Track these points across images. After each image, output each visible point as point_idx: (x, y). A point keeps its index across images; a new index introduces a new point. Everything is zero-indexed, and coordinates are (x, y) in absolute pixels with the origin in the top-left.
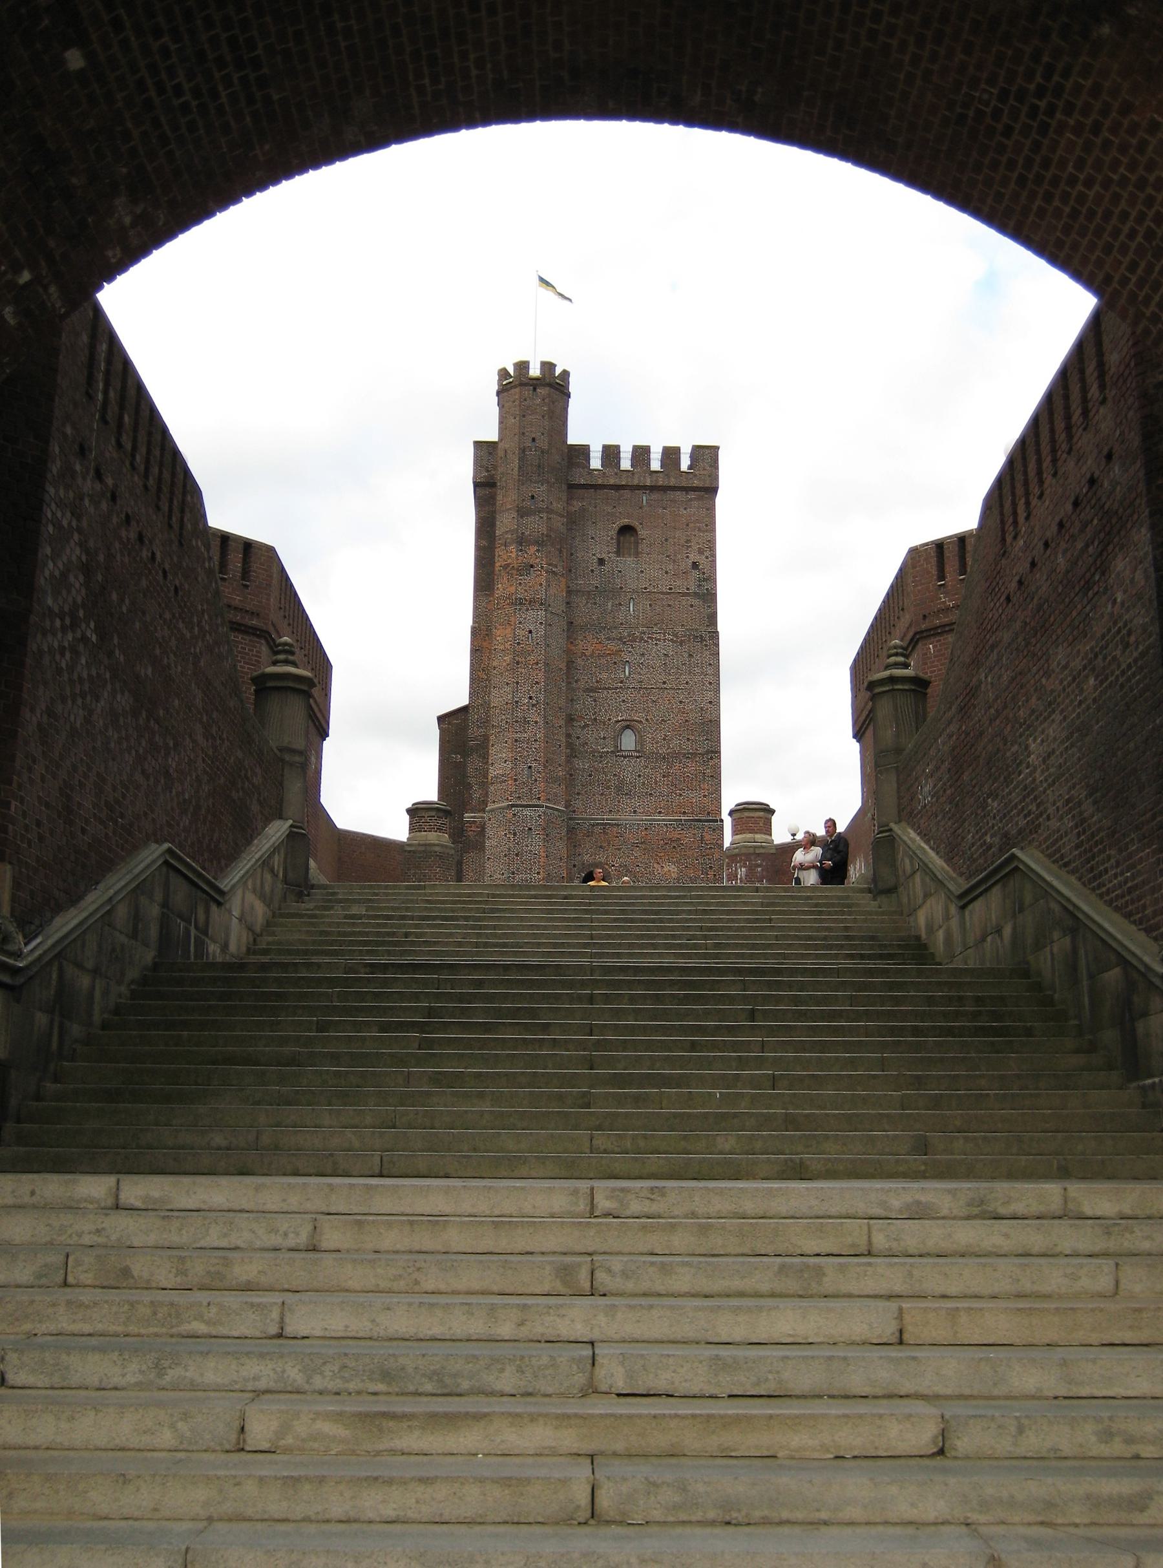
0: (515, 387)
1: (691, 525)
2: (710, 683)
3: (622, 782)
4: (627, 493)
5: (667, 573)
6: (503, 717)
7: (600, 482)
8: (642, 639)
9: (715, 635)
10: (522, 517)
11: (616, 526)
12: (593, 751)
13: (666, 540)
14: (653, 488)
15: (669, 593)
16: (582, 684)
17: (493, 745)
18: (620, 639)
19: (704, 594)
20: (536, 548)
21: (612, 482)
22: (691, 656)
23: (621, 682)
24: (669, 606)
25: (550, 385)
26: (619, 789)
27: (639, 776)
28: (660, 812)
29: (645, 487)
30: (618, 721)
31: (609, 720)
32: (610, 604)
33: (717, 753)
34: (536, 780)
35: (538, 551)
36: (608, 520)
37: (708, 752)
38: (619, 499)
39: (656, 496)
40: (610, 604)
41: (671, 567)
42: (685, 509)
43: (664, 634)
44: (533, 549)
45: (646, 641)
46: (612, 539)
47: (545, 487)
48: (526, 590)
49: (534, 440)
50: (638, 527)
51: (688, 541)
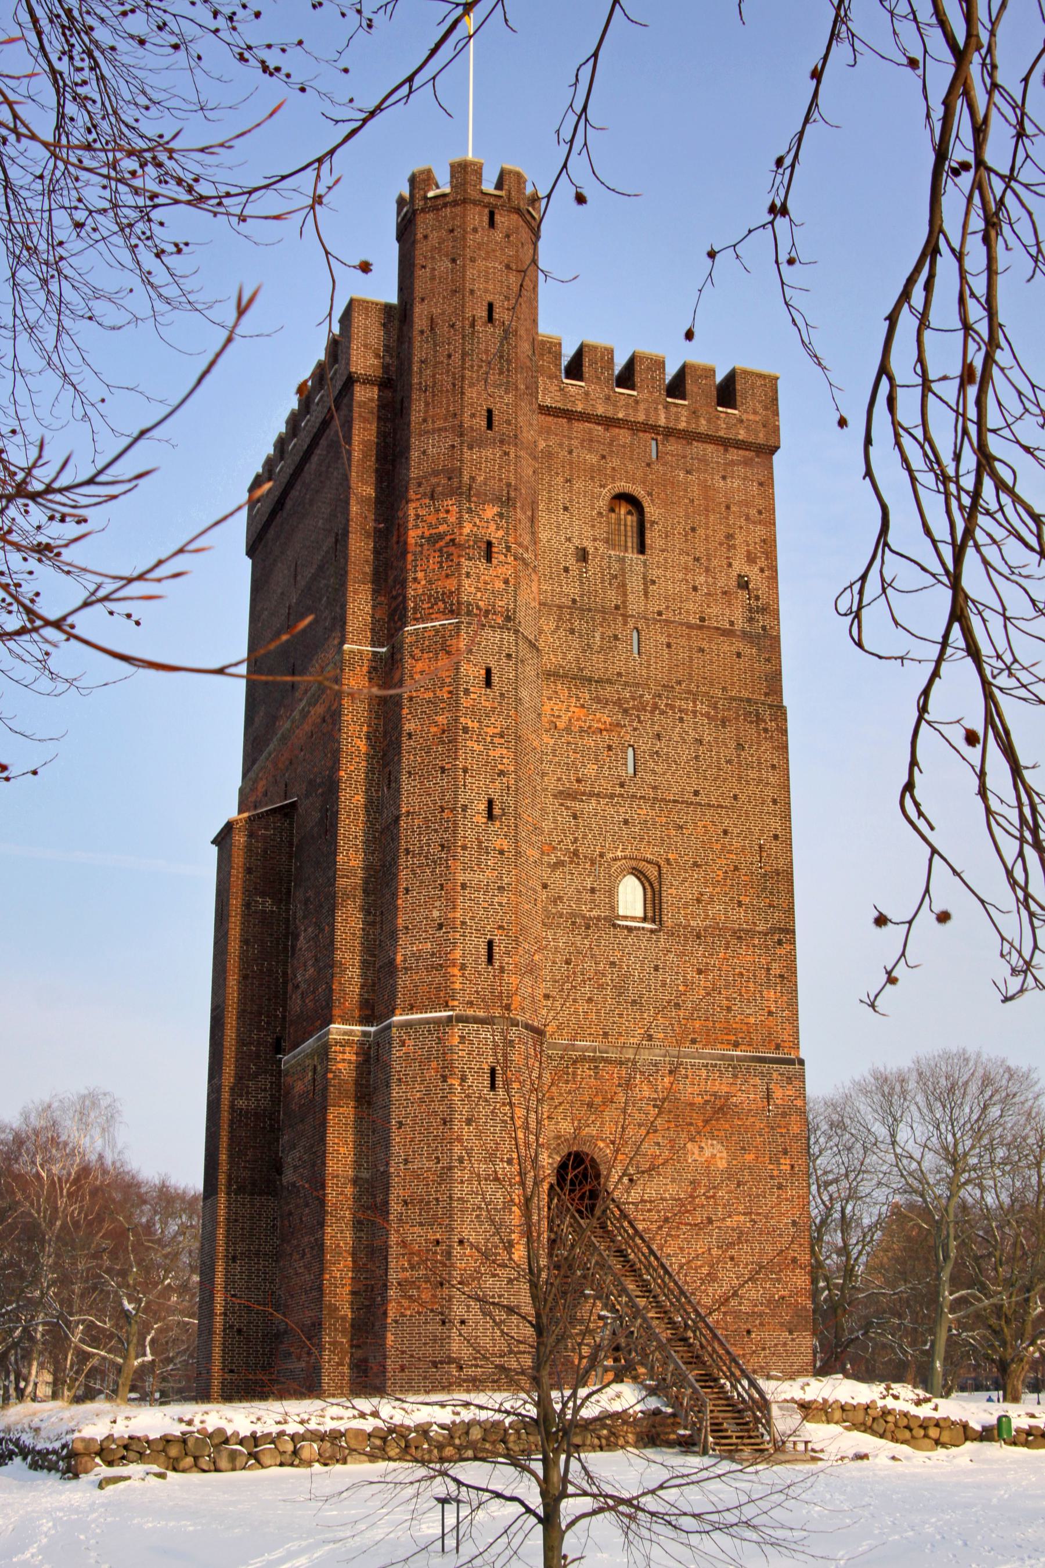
0: (455, 203)
1: (734, 508)
2: (775, 802)
3: (625, 977)
4: (624, 436)
5: (695, 589)
6: (434, 836)
7: (579, 408)
8: (655, 707)
9: (779, 713)
10: (471, 448)
11: (607, 493)
12: (573, 915)
13: (693, 529)
14: (670, 433)
15: (701, 628)
16: (551, 783)
17: (407, 890)
18: (618, 703)
20: (496, 510)
21: (600, 411)
22: (740, 747)
23: (622, 785)
24: (701, 650)
25: (518, 211)
26: (620, 990)
27: (656, 969)
28: (694, 1041)
29: (654, 429)
30: (615, 859)
31: (602, 855)
32: (597, 635)
33: (786, 933)
34: (502, 969)
35: (500, 515)
36: (592, 478)
37: (773, 931)
38: (611, 444)
39: (673, 446)
40: (597, 635)
41: (702, 579)
42: (724, 478)
43: (694, 702)
45: (662, 713)
46: (600, 514)
47: (509, 398)
48: (478, 589)
49: (490, 306)
50: (646, 502)
51: (730, 536)
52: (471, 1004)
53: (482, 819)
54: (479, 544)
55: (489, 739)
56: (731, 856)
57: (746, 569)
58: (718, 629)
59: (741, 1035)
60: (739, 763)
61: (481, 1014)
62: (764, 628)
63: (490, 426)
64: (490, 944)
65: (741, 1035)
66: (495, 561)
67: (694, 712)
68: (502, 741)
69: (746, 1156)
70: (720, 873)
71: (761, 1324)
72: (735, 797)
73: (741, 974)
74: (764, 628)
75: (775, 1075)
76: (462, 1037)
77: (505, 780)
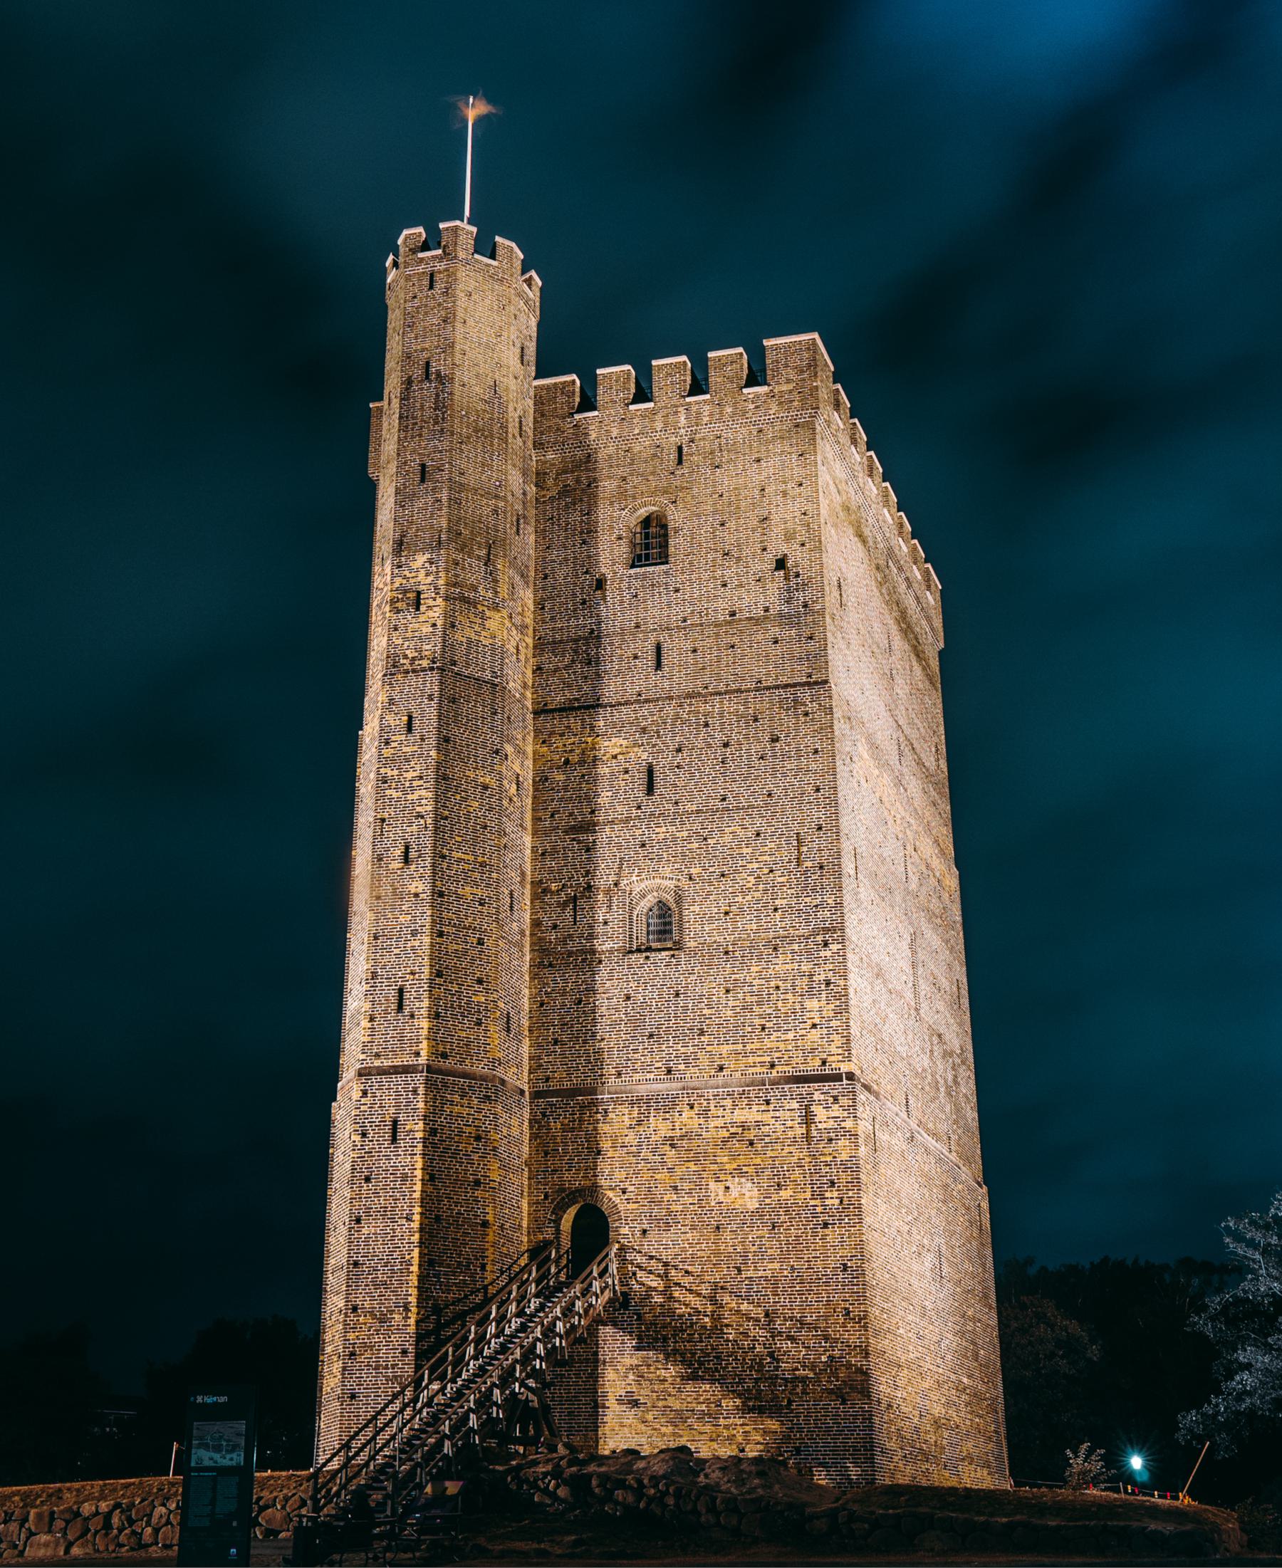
15: (729, 623)
19: (798, 615)
34: (412, 1016)
35: (431, 562)
44: (421, 559)
52: (377, 1055)
53: (396, 865)
54: (408, 595)
55: (407, 784)
56: (764, 858)
57: (784, 549)
58: (751, 619)
59: (778, 1055)
60: (774, 756)
61: (387, 1063)
62: (805, 606)
63: (423, 480)
64: (401, 991)
65: (778, 1055)
66: (423, 608)
67: (721, 714)
68: (421, 782)
69: (782, 1193)
70: (751, 879)
71: (804, 1392)
72: (769, 795)
73: (778, 988)
74: (805, 606)
75: (817, 1096)
76: (365, 1093)
77: (422, 822)
